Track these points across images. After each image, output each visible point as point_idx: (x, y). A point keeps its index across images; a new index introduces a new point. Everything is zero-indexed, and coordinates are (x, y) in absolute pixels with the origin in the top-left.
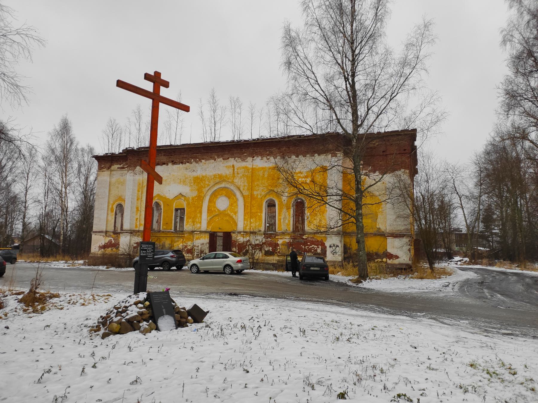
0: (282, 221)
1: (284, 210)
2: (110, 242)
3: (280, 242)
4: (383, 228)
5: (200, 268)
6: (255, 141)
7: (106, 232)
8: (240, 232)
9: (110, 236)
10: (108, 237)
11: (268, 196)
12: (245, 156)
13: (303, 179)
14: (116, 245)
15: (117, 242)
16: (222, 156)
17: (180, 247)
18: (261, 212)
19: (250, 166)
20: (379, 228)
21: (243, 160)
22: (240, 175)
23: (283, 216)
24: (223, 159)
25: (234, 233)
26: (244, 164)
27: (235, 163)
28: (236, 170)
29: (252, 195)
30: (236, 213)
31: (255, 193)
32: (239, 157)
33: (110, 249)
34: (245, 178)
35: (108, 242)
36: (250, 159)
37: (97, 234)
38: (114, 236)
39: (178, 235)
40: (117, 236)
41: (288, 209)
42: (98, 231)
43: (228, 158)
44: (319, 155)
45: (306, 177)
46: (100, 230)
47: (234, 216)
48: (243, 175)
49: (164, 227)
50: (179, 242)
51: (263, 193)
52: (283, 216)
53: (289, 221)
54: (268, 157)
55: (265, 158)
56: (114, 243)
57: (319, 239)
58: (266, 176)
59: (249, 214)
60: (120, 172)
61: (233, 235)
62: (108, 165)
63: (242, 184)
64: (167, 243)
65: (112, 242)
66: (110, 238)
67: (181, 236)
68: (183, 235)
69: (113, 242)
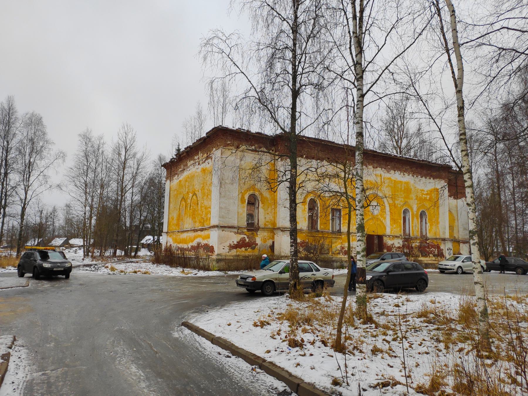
0: (414, 228)
1: (415, 219)
2: (243, 240)
3: (413, 245)
4: (457, 237)
5: (464, 269)
6: (401, 158)
7: (239, 228)
8: (389, 236)
9: (242, 233)
10: (240, 234)
11: (404, 206)
12: (389, 168)
13: (425, 196)
14: (252, 245)
15: (253, 241)
16: (372, 164)
17: (338, 248)
18: (400, 219)
19: (393, 178)
20: (455, 237)
21: (388, 172)
22: (386, 185)
23: (414, 225)
24: (373, 167)
25: (386, 236)
26: (387, 175)
27: (382, 173)
28: (383, 180)
29: (395, 204)
30: (385, 218)
31: (396, 202)
32: (385, 169)
33: (243, 249)
34: (390, 188)
35: (240, 240)
36: (392, 172)
37: (226, 229)
38: (248, 233)
39: (336, 236)
40: (253, 234)
41: (417, 219)
42: (226, 225)
43: (377, 168)
44: (433, 179)
45: (427, 194)
46: (230, 225)
47: (384, 221)
48: (388, 185)
49: (322, 227)
50: (337, 243)
51: (402, 203)
52: (414, 225)
53: (418, 228)
54: (405, 173)
55: (402, 174)
56: (248, 242)
57: (436, 244)
58: (403, 189)
59: (393, 220)
60: (251, 155)
61: (385, 238)
62: (236, 143)
63: (387, 192)
64: (327, 242)
65: (245, 240)
66: (242, 236)
67: (338, 237)
68: (340, 237)
69: (247, 240)
